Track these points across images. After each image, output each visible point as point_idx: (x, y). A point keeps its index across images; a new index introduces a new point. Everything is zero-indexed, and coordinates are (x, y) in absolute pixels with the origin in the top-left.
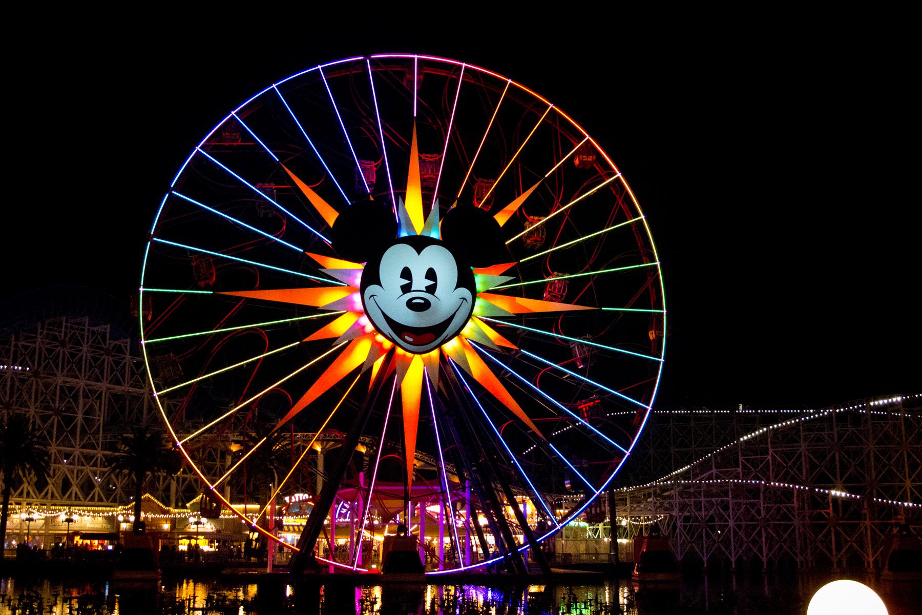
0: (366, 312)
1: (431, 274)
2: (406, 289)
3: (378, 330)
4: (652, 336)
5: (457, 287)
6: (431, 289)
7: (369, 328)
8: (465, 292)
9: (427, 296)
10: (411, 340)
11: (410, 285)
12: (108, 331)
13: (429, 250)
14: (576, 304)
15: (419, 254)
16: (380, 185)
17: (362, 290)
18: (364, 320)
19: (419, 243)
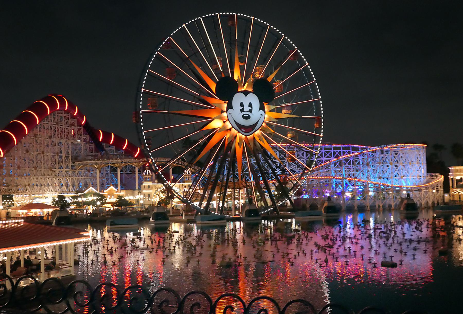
0: (228, 120)
1: (250, 105)
2: (242, 111)
3: (233, 127)
4: (316, 125)
5: (259, 110)
6: (251, 111)
7: (229, 126)
8: (262, 112)
9: (249, 113)
10: (244, 130)
11: (243, 109)
12: (70, 116)
13: (249, 95)
14: (293, 114)
15: (246, 96)
16: (225, 66)
17: (227, 112)
18: (228, 123)
19: (246, 93)
